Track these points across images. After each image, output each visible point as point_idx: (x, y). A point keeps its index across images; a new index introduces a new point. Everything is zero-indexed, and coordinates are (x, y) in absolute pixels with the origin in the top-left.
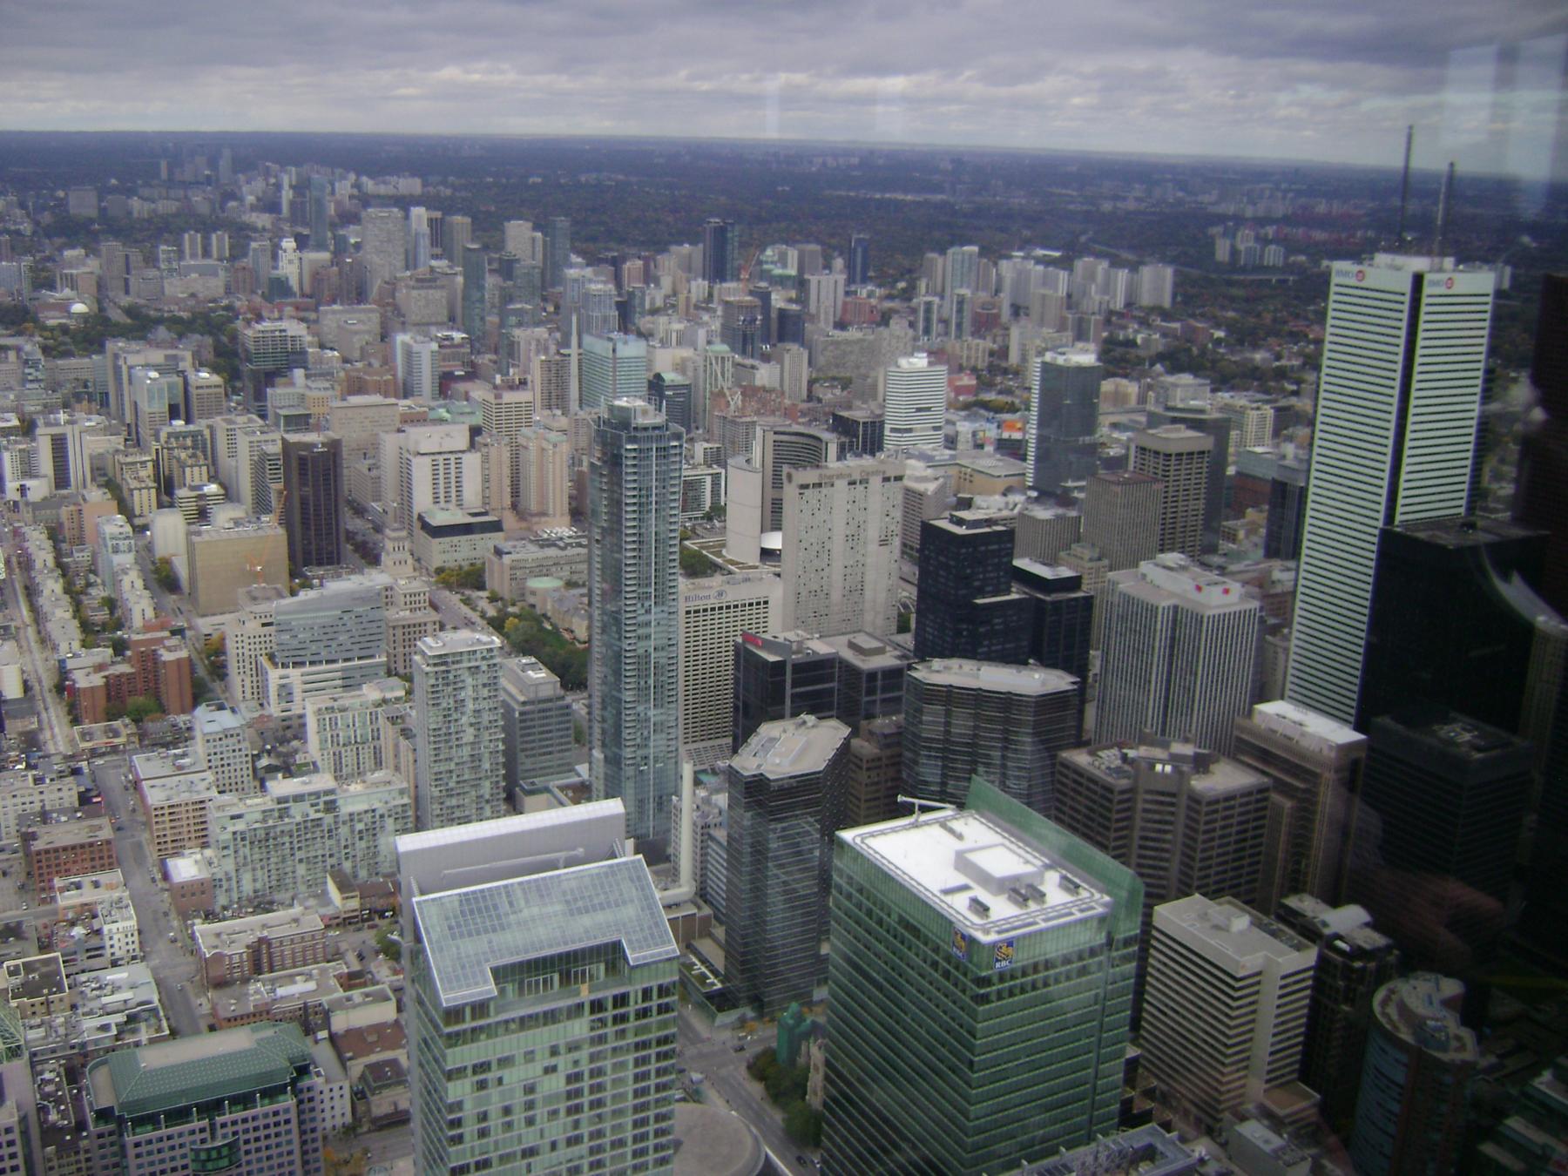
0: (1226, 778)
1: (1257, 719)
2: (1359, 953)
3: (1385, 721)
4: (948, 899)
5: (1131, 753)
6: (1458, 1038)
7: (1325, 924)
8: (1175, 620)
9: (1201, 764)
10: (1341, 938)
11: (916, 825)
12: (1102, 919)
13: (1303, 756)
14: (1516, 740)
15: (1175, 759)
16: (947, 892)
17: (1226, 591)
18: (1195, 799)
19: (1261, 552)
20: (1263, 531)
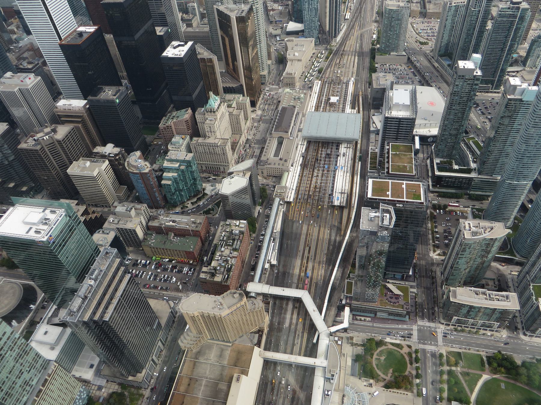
0: (62, 131)
1: (59, 108)
2: (116, 155)
3: (90, 98)
4: (29, 234)
5: (36, 138)
6: (146, 165)
7: (106, 153)
8: (21, 92)
9: (54, 131)
10: (110, 154)
11: (6, 218)
12: (66, 215)
13: (76, 113)
14: (121, 88)
15: (47, 134)
16: (27, 232)
17: (30, 79)
18: (59, 142)
19: (25, 34)
20: (21, 26)
